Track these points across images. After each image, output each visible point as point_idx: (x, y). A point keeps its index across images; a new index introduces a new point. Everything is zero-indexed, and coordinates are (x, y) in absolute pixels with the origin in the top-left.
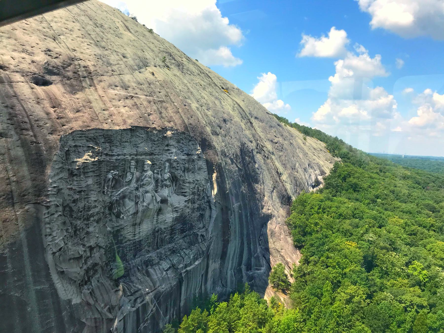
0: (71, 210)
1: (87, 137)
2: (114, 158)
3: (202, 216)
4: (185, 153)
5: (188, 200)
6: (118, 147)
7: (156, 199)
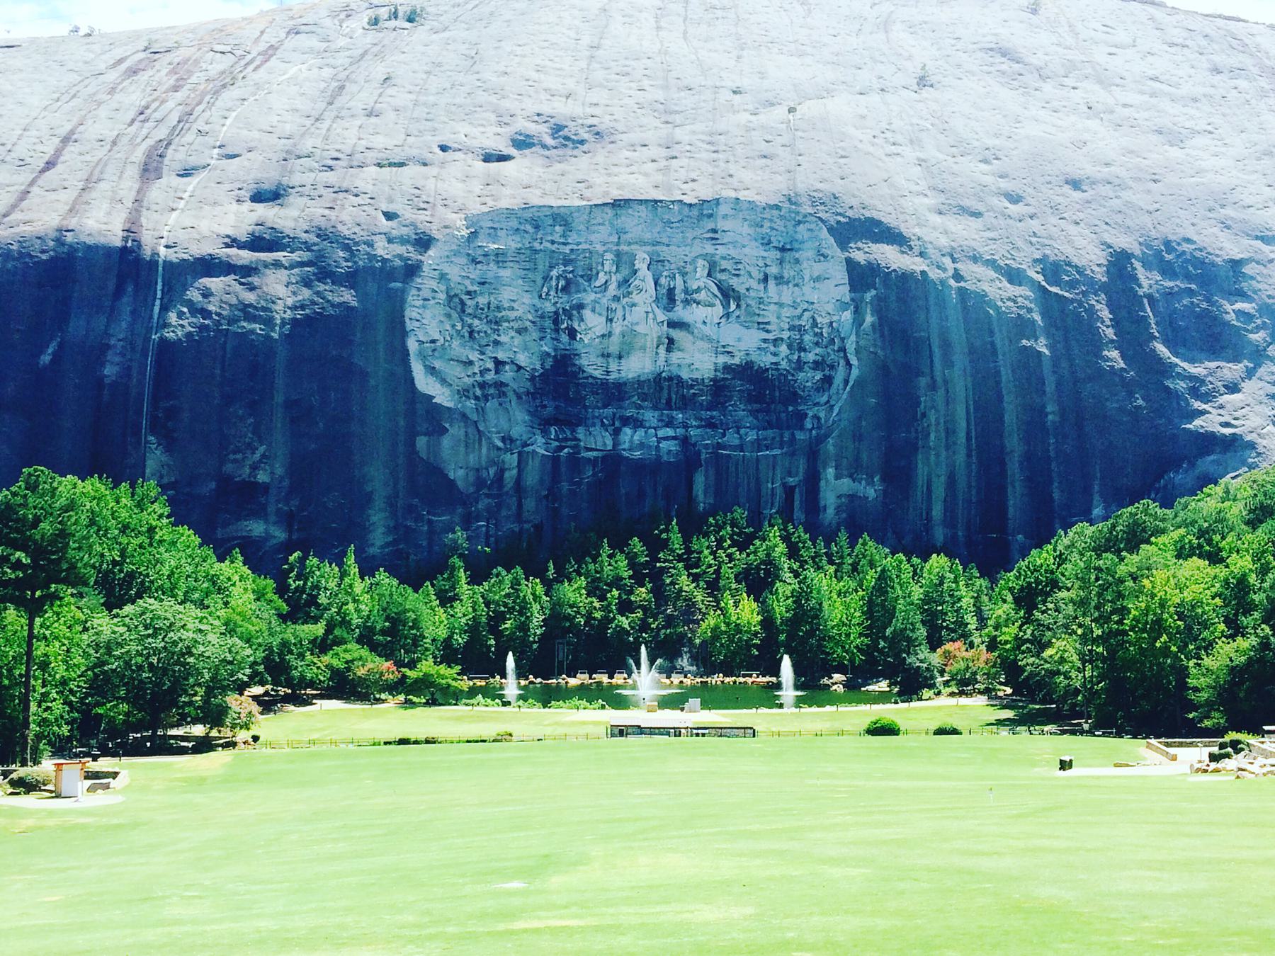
0: (463, 303)
3: (828, 380)
5: (775, 340)
7: (655, 319)
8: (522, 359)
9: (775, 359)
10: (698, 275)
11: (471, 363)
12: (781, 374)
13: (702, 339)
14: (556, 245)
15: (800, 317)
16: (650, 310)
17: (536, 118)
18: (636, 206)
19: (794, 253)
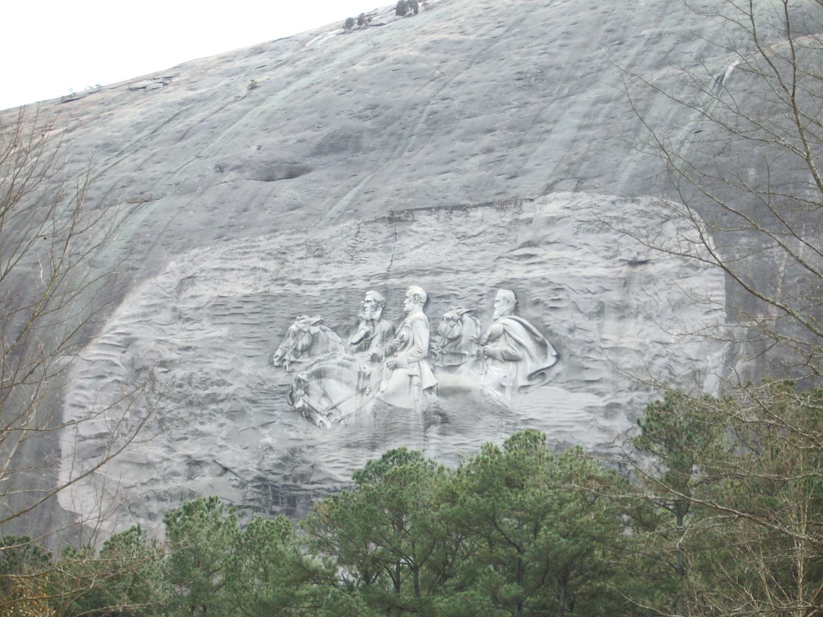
0: (153, 379)
1: (263, 251)
2: (320, 287)
4: (621, 260)
6: (343, 265)
7: (419, 385)
8: (232, 456)
9: (603, 438)
10: (496, 314)
11: (149, 465)
12: (613, 463)
13: (492, 413)
14: (303, 287)
15: (647, 368)
16: (415, 371)
17: (368, 112)
18: (423, 217)
19: (651, 269)
